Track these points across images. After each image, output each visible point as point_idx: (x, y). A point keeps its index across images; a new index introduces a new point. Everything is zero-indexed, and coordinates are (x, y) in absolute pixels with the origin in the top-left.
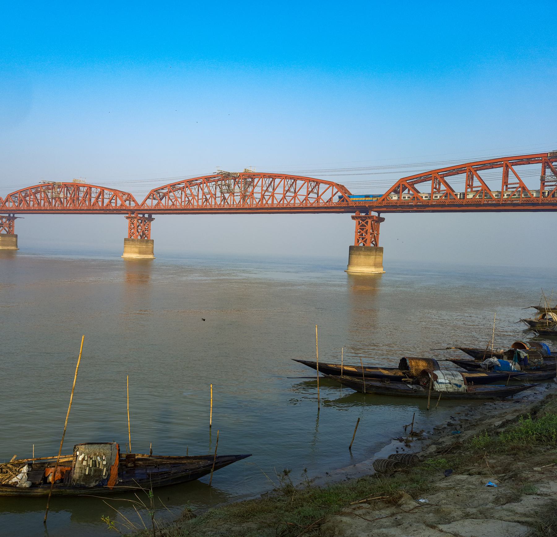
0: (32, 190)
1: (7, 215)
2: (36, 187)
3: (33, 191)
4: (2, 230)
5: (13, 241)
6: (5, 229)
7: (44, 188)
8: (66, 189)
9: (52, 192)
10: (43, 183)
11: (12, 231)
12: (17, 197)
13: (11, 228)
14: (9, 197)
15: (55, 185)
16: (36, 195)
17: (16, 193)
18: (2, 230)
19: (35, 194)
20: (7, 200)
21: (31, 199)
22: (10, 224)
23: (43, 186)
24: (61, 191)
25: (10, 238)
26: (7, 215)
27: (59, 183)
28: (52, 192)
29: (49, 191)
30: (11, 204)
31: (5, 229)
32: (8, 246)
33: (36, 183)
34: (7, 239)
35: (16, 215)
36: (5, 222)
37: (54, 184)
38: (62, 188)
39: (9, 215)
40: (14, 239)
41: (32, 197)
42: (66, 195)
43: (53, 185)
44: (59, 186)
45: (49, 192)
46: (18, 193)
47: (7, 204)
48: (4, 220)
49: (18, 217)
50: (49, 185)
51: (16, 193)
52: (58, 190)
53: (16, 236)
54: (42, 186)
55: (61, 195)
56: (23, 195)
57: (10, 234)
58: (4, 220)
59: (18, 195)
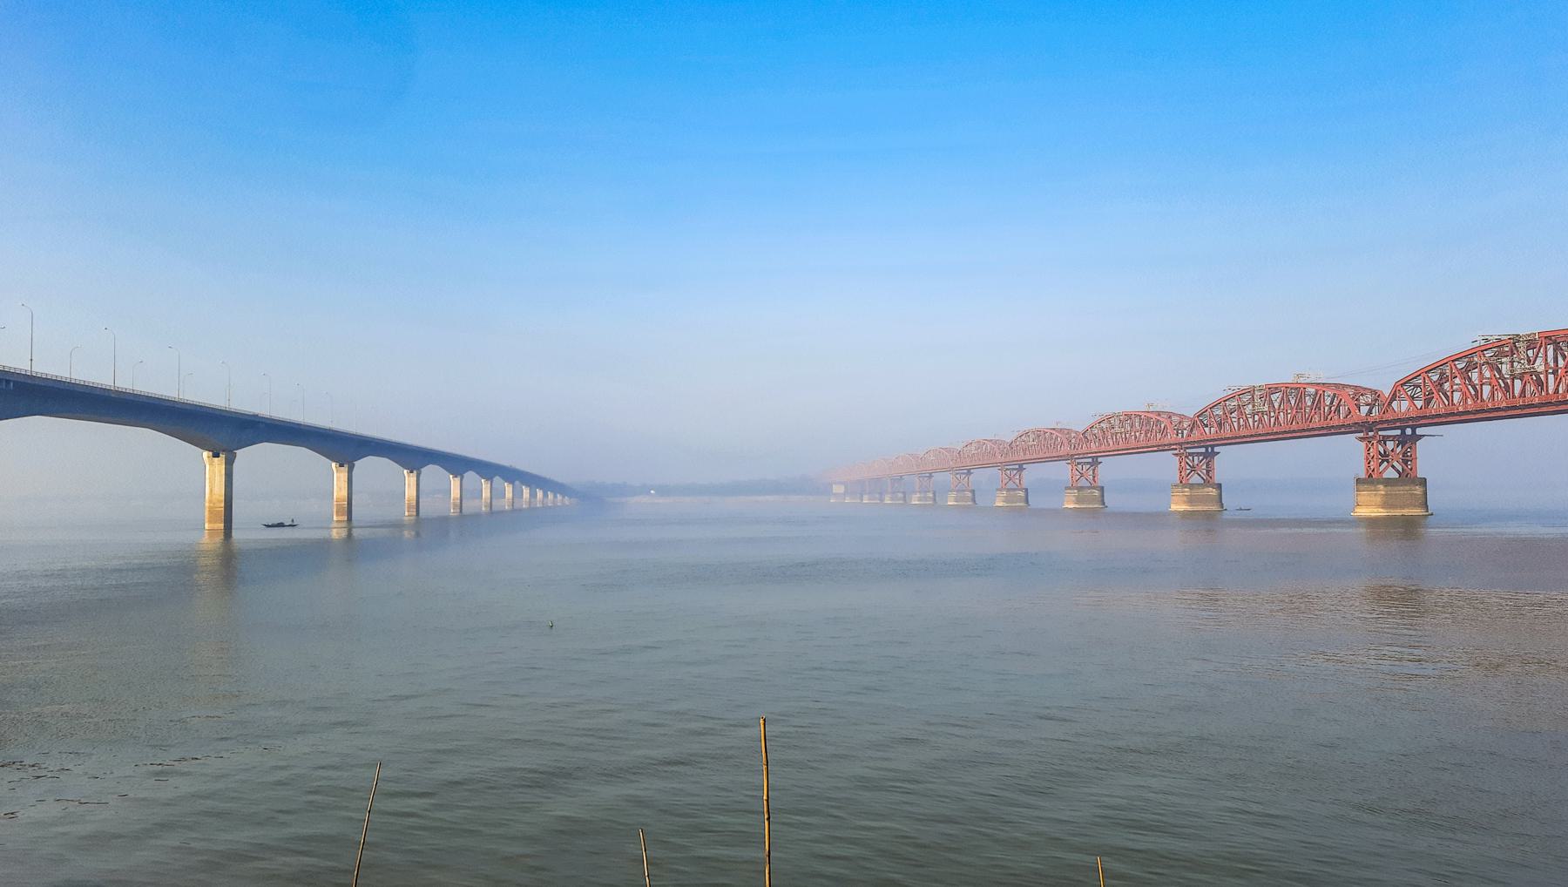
0: (1457, 363)
1: (1398, 432)
2: (1467, 355)
3: (1459, 367)
4: (1385, 469)
5: (1416, 494)
6: (1393, 467)
7: (1489, 354)
8: (1551, 348)
9: (1512, 362)
10: (1483, 343)
11: (1411, 470)
12: (1419, 386)
13: (1409, 463)
14: (1400, 388)
15: (1519, 341)
16: (1470, 374)
17: (1415, 378)
18: (1385, 469)
19: (1467, 369)
20: (1394, 397)
21: (1455, 387)
22: (1405, 454)
23: (1486, 350)
24: (1537, 356)
25: (1407, 488)
26: (1398, 432)
27: (1529, 336)
28: (1512, 362)
29: (1504, 360)
30: (1405, 405)
31: (1393, 467)
32: (1402, 507)
33: (1463, 344)
34: (1400, 490)
35: (1419, 431)
36: (1392, 450)
37: (1515, 339)
38: (1541, 347)
39: (1403, 432)
40: (1418, 490)
41: (1457, 381)
42: (1552, 364)
43: (1514, 343)
44: (1531, 343)
45: (1501, 363)
46: (1420, 375)
47: (1395, 404)
48: (1390, 445)
49: (1424, 436)
50: (1499, 344)
51: (1415, 378)
52: (1530, 353)
53: (1423, 482)
54: (1482, 351)
55: (1539, 366)
56: (1435, 378)
57: (1408, 477)
58: (1390, 445)
59: (1420, 381)
